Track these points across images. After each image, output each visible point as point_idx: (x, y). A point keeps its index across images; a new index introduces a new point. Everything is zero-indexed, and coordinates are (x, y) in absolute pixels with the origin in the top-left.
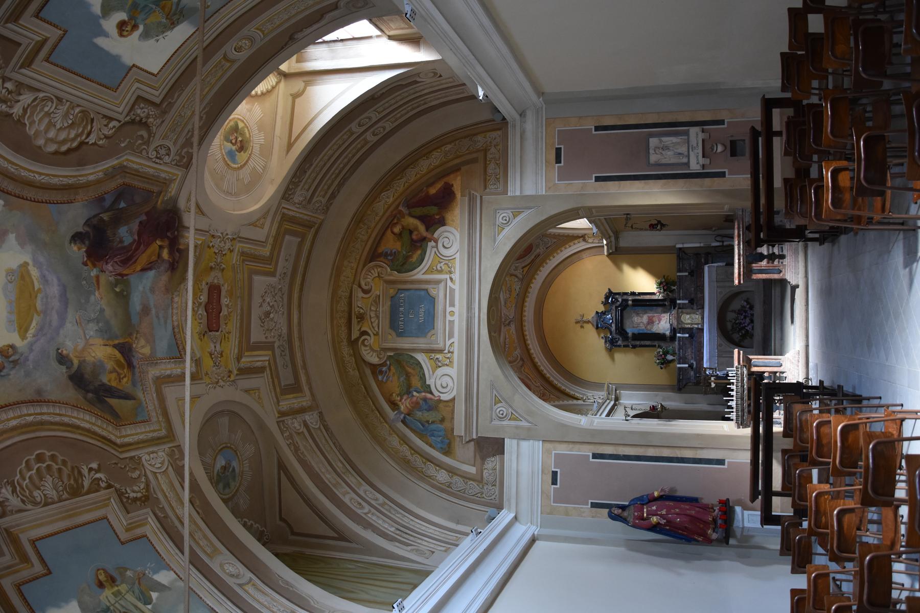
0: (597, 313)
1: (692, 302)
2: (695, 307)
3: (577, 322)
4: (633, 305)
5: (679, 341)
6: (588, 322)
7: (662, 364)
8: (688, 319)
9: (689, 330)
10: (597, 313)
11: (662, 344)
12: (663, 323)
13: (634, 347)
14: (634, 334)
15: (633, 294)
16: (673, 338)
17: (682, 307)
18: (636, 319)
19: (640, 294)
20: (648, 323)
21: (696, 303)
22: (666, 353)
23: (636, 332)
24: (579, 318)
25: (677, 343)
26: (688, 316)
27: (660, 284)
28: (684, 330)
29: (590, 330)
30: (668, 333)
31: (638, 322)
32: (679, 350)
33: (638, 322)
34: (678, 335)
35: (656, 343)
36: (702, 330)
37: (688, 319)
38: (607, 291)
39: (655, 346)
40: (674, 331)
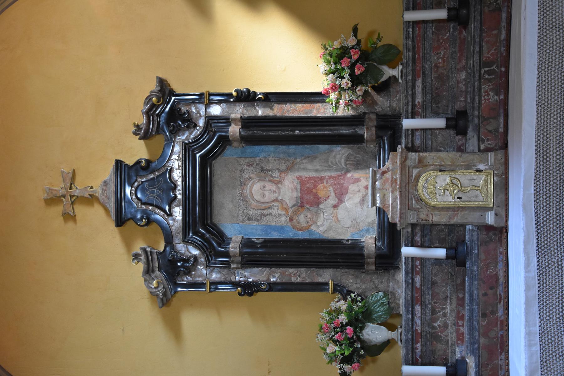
0: (119, 164)
1: (458, 123)
2: (472, 143)
3: (52, 200)
4: (246, 140)
5: (411, 272)
6: (91, 199)
7: (347, 360)
8: (442, 189)
9: (452, 236)
10: (119, 164)
11: (350, 280)
12: (352, 207)
13: (249, 289)
14: (247, 243)
15: (246, 97)
16: (387, 259)
17: (422, 143)
18: (258, 190)
19: (270, 98)
20: (301, 205)
21: (476, 125)
22: (359, 320)
23: (257, 233)
24: (59, 187)
25: (401, 276)
26: (444, 179)
27: (338, 58)
28: (425, 234)
29: (97, 221)
30: (369, 241)
31: (263, 198)
32: (411, 303)
33: (263, 198)
34: (407, 251)
35: (326, 276)
36: (501, 232)
37: (442, 189)
38: (153, 86)
39: (320, 287)
40: (390, 234)
